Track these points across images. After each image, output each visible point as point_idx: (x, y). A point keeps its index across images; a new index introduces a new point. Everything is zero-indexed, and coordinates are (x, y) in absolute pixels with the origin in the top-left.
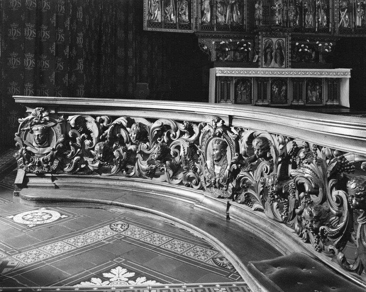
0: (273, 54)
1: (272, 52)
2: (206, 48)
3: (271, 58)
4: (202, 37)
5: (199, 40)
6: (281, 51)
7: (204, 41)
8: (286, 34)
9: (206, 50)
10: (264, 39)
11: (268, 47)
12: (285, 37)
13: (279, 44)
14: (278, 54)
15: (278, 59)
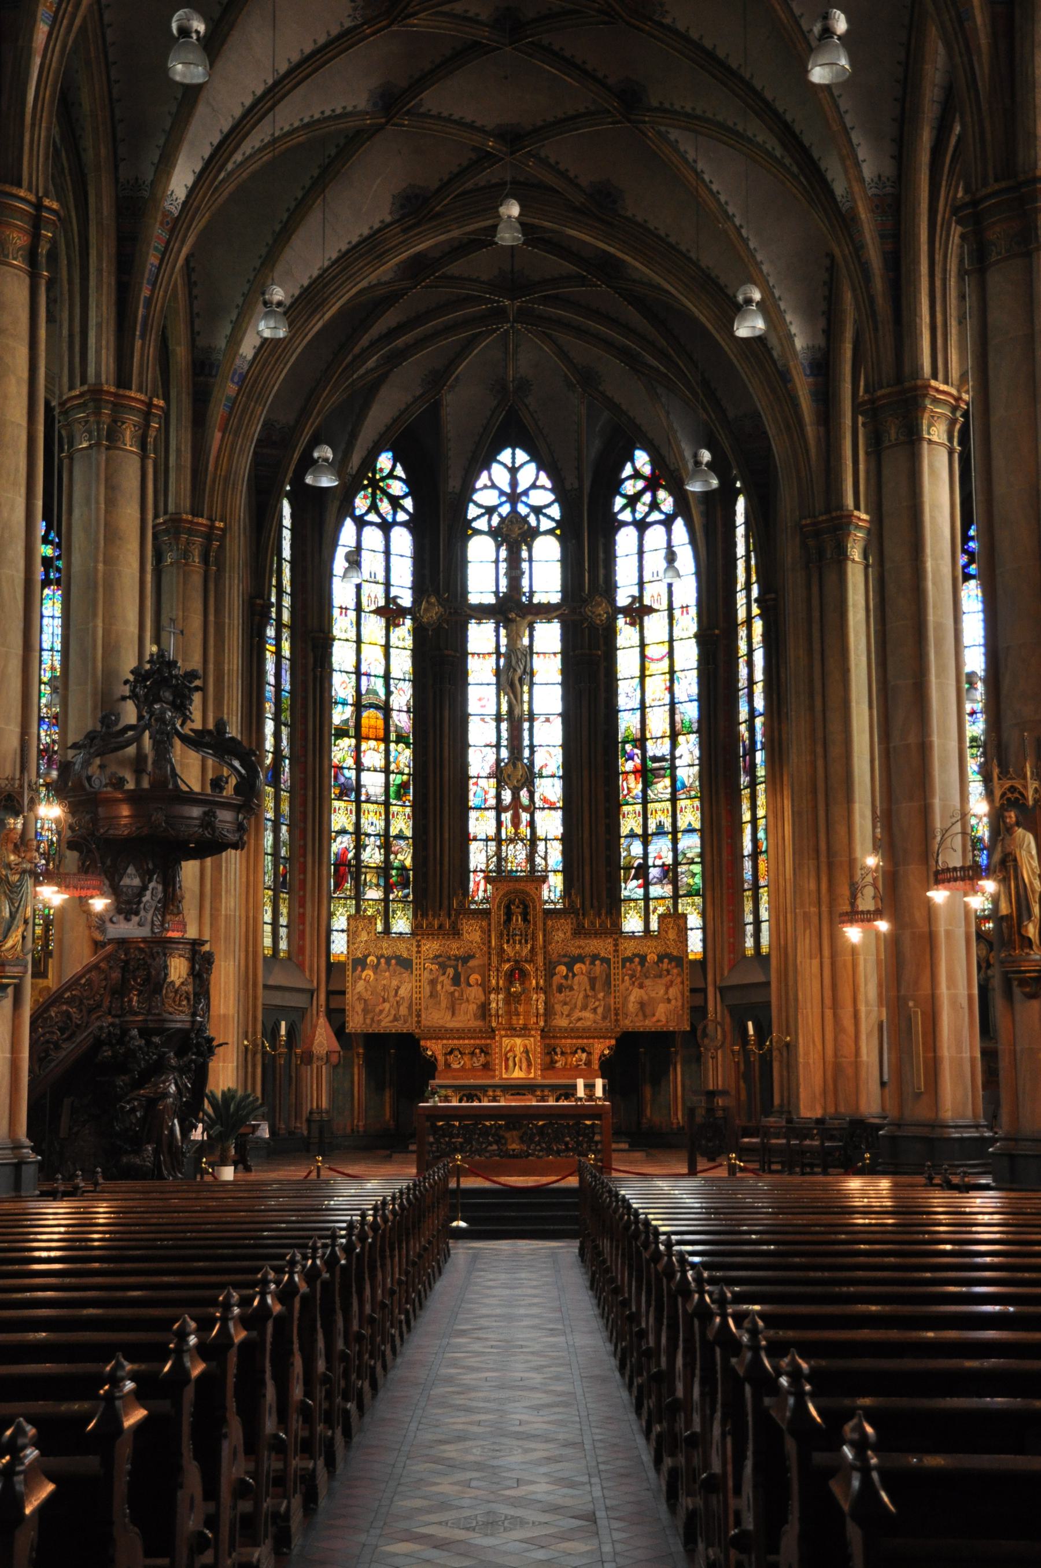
0: (517, 1059)
1: (515, 1057)
2: (429, 1053)
3: (515, 1065)
4: (426, 1039)
5: (422, 1043)
6: (528, 1055)
7: (428, 1043)
8: (533, 1032)
9: (431, 1056)
10: (504, 1039)
11: (510, 1050)
12: (533, 1036)
13: (525, 1046)
14: (524, 1060)
15: (524, 1066)
